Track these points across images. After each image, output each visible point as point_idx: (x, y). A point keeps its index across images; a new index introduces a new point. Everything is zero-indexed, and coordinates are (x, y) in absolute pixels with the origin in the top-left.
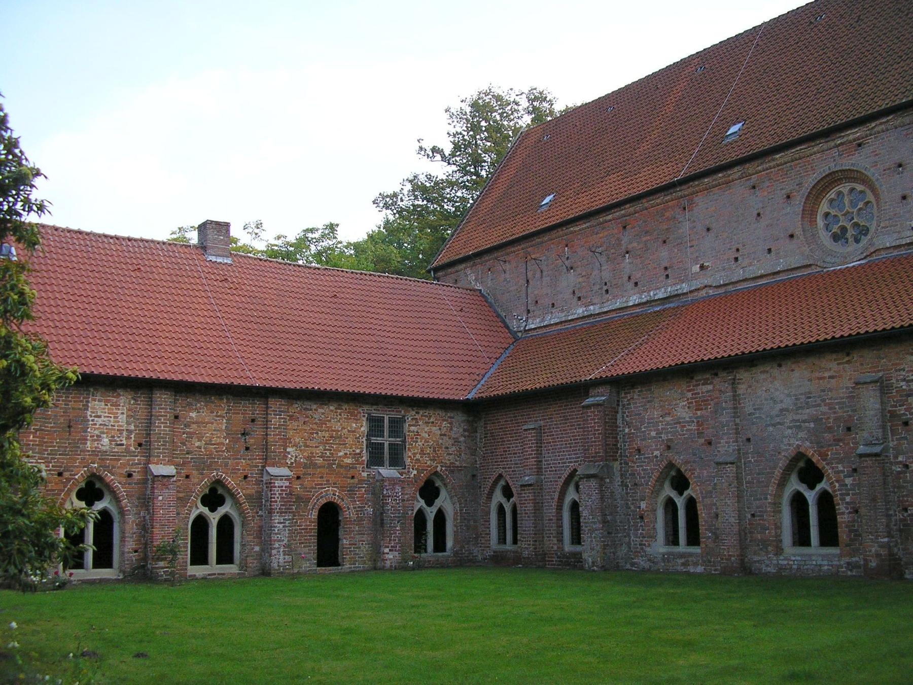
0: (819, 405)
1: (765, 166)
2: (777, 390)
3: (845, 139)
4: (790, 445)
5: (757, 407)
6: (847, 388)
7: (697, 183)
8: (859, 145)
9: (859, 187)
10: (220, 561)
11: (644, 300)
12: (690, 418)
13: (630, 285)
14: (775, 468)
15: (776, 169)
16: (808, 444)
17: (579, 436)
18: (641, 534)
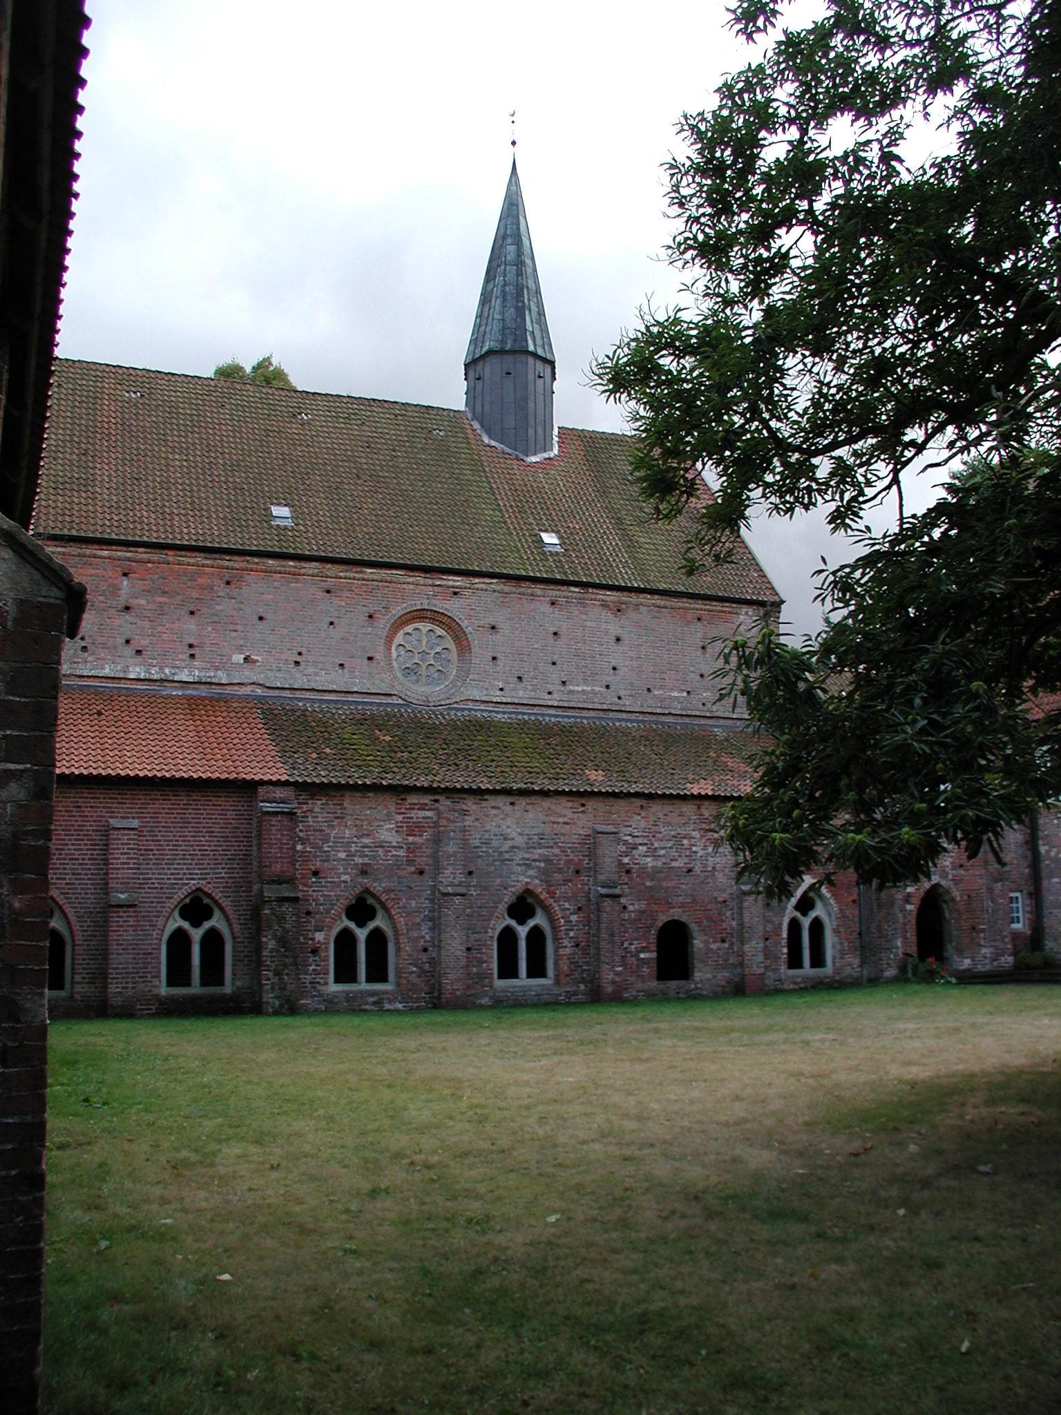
0: (552, 847)
1: (349, 574)
2: (508, 827)
3: (444, 583)
4: (518, 881)
5: (531, 845)
6: (580, 835)
7: (256, 560)
8: (455, 593)
9: (440, 631)
10: (813, 965)
11: (156, 677)
12: (398, 843)
13: (129, 651)
14: (500, 902)
15: (360, 583)
16: (537, 882)
17: (209, 846)
18: (314, 970)
